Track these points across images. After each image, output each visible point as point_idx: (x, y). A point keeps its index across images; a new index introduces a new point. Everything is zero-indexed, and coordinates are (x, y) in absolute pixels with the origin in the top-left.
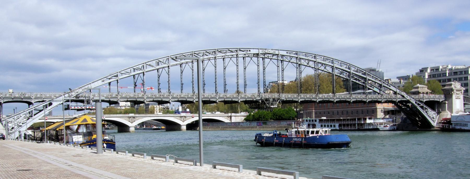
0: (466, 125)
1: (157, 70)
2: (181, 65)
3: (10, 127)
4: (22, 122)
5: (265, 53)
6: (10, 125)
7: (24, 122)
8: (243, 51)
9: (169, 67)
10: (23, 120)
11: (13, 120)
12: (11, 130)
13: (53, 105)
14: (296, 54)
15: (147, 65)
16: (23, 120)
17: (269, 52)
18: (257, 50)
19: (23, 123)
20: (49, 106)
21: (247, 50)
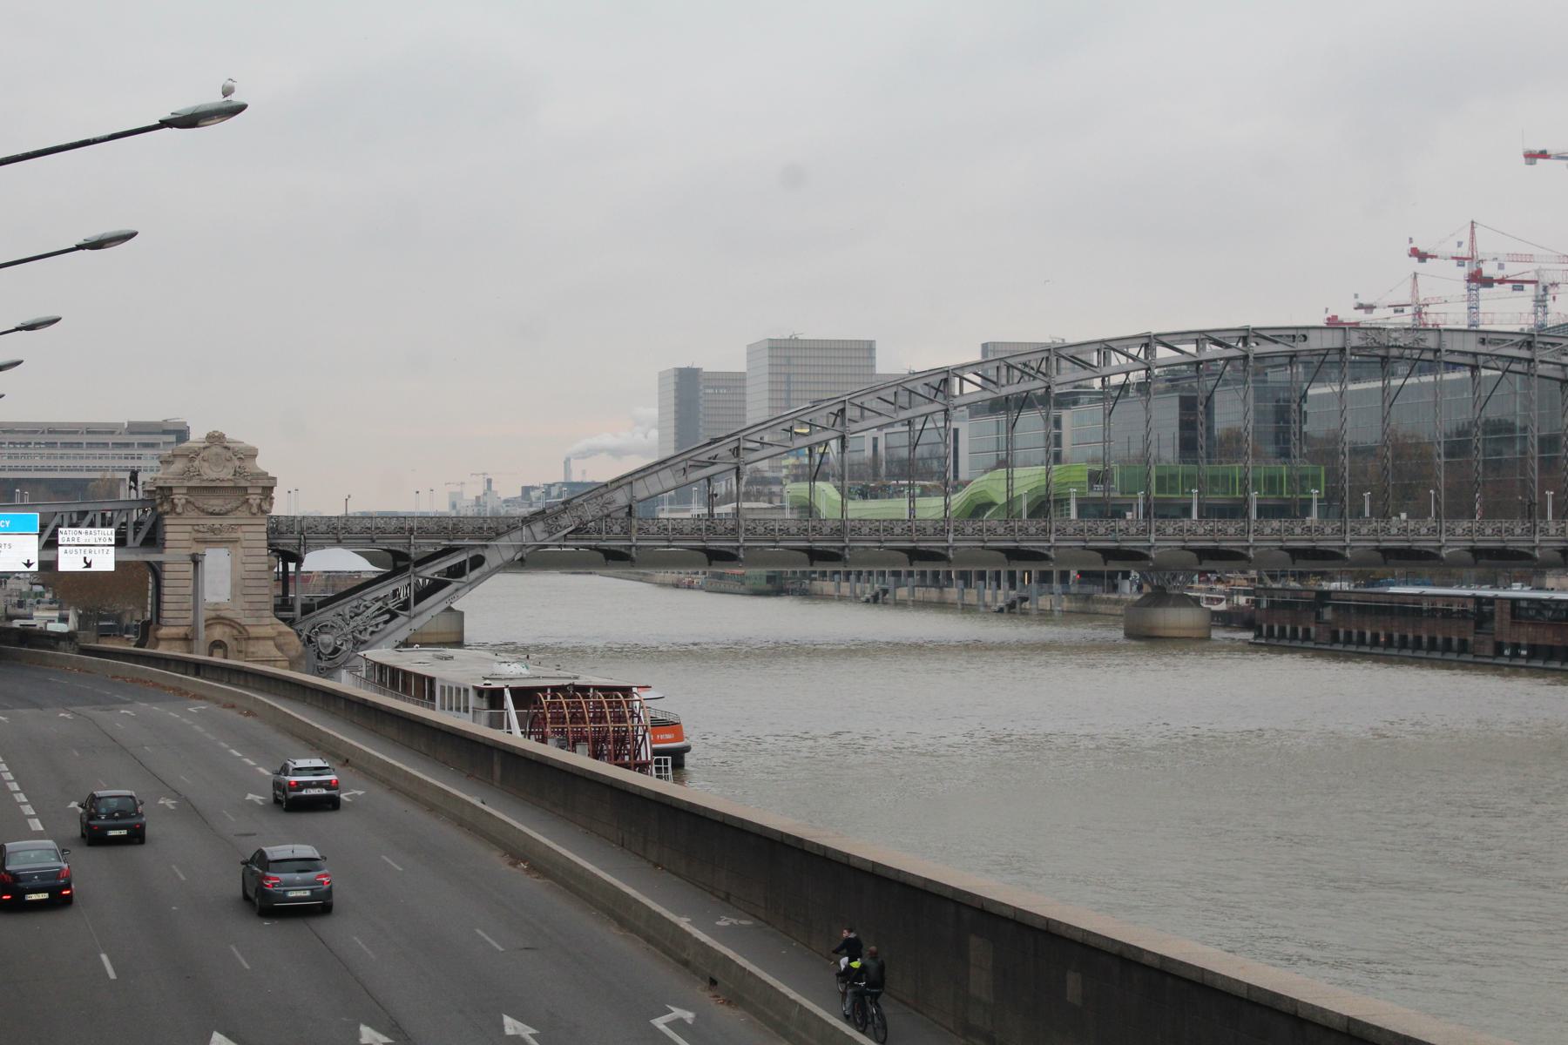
0: (1355, 638)
1: (1101, 379)
2: (910, 422)
3: (326, 646)
4: (371, 629)
5: (1375, 345)
6: (326, 638)
7: (376, 630)
8: (1276, 342)
9: (946, 411)
10: (374, 622)
11: (339, 620)
12: (330, 659)
13: (486, 565)
14: (1529, 345)
15: (1063, 357)
16: (374, 622)
17: (1396, 340)
18: (1338, 334)
19: (373, 633)
20: (472, 569)
21: (1294, 336)
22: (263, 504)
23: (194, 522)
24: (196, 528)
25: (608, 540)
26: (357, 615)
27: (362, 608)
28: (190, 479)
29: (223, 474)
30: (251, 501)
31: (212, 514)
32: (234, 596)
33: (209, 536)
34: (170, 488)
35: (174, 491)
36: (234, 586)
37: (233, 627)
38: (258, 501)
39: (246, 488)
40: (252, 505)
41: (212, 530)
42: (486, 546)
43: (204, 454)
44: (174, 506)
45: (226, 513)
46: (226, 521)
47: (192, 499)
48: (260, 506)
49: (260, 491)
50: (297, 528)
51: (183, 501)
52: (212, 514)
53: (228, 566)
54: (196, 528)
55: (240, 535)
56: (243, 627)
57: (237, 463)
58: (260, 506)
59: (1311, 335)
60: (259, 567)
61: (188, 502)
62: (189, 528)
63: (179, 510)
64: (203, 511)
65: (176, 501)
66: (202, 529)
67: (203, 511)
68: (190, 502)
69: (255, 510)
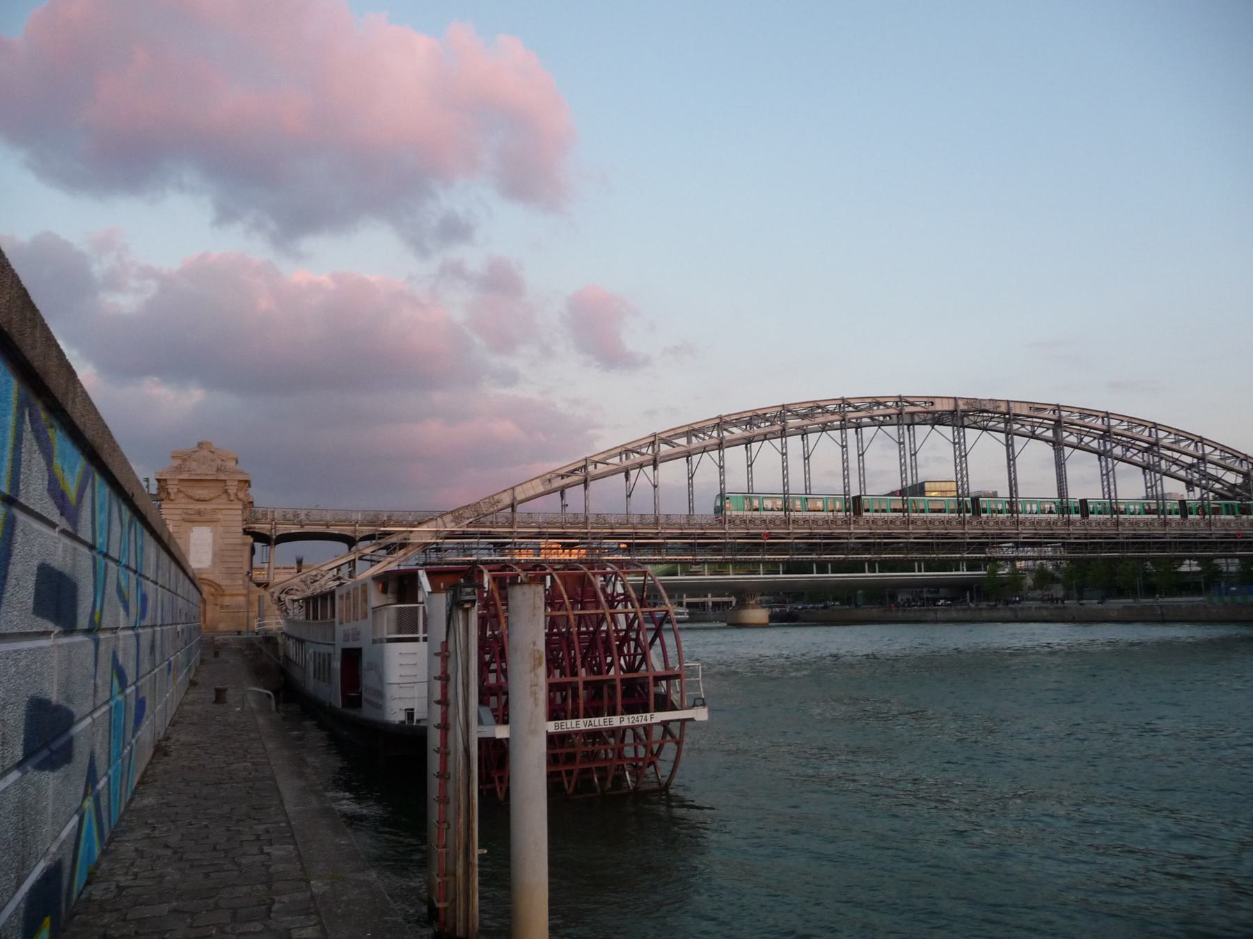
22: (239, 493)
23: (183, 506)
24: (185, 511)
25: (497, 527)
26: (315, 581)
27: (319, 577)
28: (181, 473)
29: (206, 471)
30: (229, 491)
31: (198, 500)
32: (214, 563)
33: (197, 518)
34: (165, 480)
35: (169, 482)
36: (215, 555)
37: (211, 586)
38: (235, 491)
39: (225, 481)
40: (229, 495)
41: (199, 513)
42: (411, 532)
43: (196, 456)
44: (169, 494)
45: (211, 500)
46: (209, 506)
47: (182, 489)
48: (236, 495)
49: (236, 483)
50: (269, 516)
51: (176, 490)
52: (198, 500)
53: (210, 540)
54: (185, 511)
55: (221, 517)
56: (219, 586)
57: (219, 462)
58: (236, 495)
59: (937, 401)
60: (233, 541)
61: (179, 491)
62: (180, 512)
63: (172, 497)
64: (191, 498)
65: (169, 490)
66: (190, 512)
67: (191, 498)
68: (181, 492)
69: (232, 497)
